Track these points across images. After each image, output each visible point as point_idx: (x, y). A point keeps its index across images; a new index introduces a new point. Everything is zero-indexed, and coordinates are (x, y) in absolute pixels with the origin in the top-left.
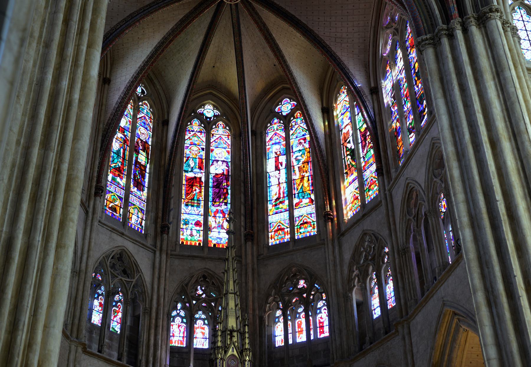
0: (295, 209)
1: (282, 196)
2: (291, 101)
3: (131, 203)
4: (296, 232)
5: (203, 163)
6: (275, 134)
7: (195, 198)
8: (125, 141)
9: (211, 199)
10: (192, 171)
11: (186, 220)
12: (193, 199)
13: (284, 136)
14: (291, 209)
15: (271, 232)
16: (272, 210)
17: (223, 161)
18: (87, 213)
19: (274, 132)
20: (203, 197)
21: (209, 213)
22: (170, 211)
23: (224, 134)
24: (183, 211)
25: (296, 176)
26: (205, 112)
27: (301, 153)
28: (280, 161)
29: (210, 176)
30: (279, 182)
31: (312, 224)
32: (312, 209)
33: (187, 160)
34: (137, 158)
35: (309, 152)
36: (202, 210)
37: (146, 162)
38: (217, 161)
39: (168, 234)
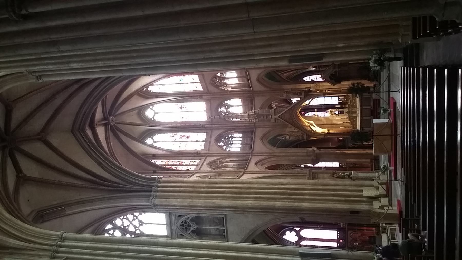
18: (208, 156)
22: (196, 125)
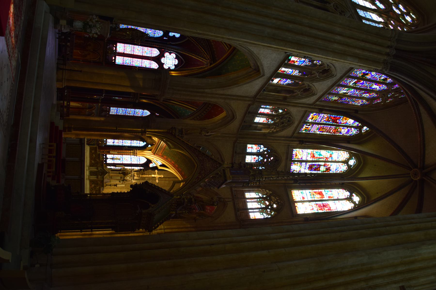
3: (301, 164)
7: (314, 196)
8: (327, 158)
9: (317, 203)
10: (326, 194)
18: (291, 137)
34: (322, 165)
37: (322, 171)
39: (294, 183)
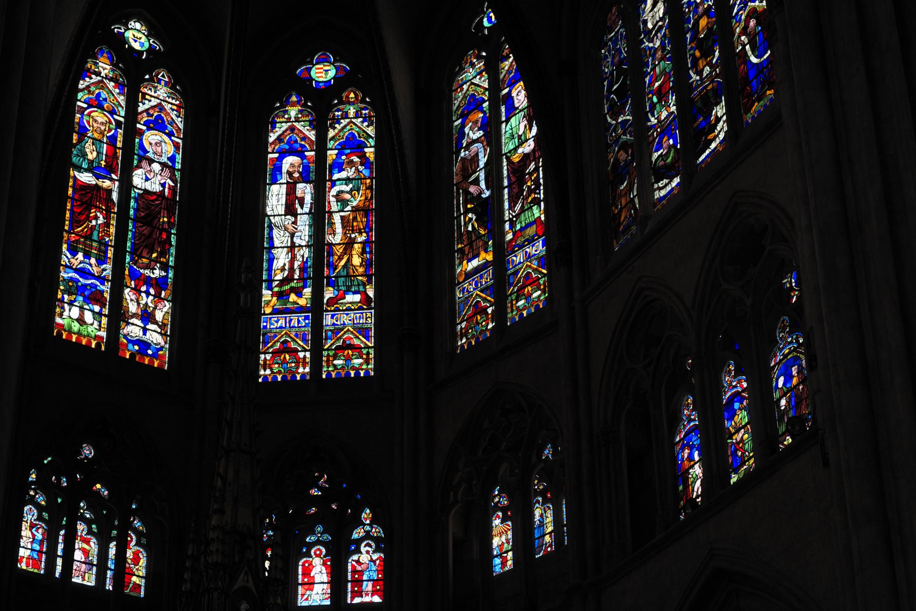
0: (327, 311)
1: (296, 277)
2: (335, 61)
4: (324, 364)
5: (117, 158)
6: (292, 129)
7: (95, 237)
11: (71, 284)
12: (88, 237)
13: (313, 138)
14: (317, 308)
15: (265, 353)
16: (272, 304)
17: (163, 165)
19: (289, 124)
20: (112, 238)
21: (124, 278)
23: (170, 100)
24: (64, 260)
25: (337, 238)
26: (129, 34)
27: (351, 186)
28: (299, 193)
29: (133, 192)
30: (293, 243)
31: (365, 351)
32: (368, 319)
33: (80, 140)
35: (370, 188)
36: (108, 267)
38: (151, 161)
